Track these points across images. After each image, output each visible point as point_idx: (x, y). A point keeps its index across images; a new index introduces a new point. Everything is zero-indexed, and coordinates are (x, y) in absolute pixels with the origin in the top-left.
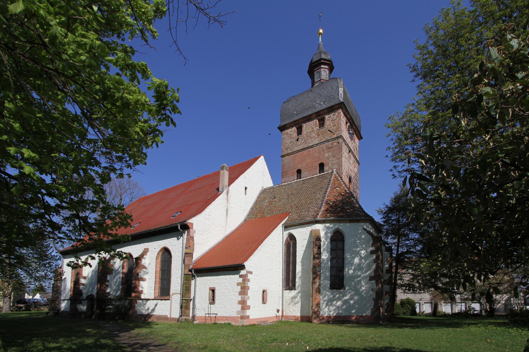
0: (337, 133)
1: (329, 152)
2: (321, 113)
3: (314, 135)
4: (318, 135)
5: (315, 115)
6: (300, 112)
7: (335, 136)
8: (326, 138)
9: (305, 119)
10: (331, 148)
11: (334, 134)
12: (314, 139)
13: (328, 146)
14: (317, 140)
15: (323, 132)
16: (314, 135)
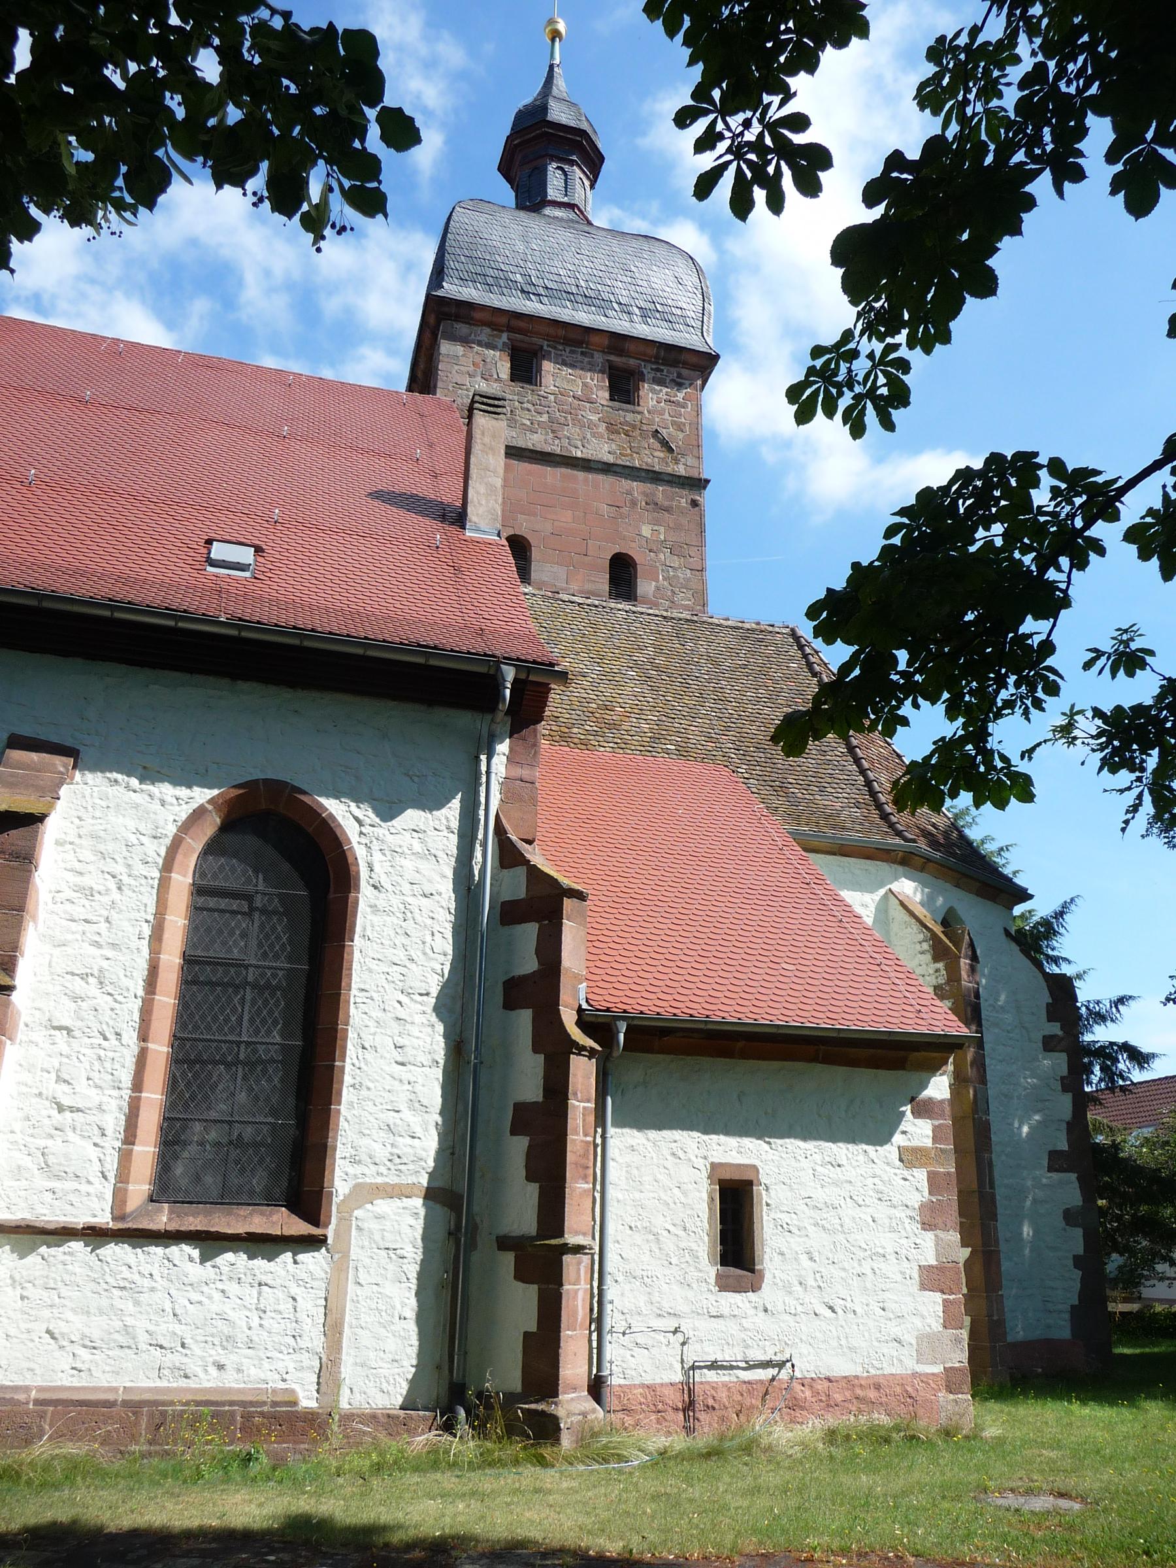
0: (690, 461)
1: (657, 522)
2: (628, 345)
3: (594, 418)
4: (612, 428)
5: (606, 341)
6: (541, 291)
7: (681, 470)
8: (646, 459)
9: (561, 332)
10: (667, 510)
11: (677, 461)
12: (594, 435)
13: (654, 495)
14: (606, 447)
15: (634, 427)
16: (594, 418)
